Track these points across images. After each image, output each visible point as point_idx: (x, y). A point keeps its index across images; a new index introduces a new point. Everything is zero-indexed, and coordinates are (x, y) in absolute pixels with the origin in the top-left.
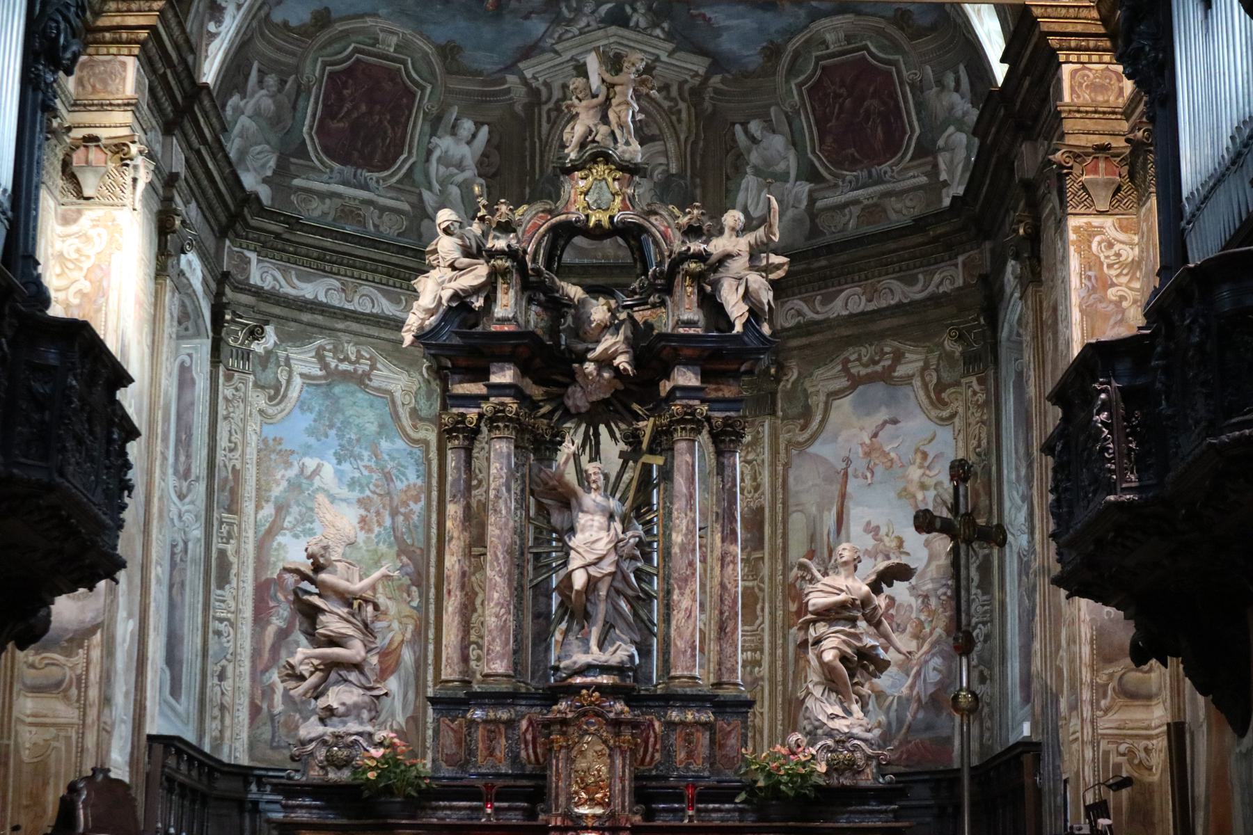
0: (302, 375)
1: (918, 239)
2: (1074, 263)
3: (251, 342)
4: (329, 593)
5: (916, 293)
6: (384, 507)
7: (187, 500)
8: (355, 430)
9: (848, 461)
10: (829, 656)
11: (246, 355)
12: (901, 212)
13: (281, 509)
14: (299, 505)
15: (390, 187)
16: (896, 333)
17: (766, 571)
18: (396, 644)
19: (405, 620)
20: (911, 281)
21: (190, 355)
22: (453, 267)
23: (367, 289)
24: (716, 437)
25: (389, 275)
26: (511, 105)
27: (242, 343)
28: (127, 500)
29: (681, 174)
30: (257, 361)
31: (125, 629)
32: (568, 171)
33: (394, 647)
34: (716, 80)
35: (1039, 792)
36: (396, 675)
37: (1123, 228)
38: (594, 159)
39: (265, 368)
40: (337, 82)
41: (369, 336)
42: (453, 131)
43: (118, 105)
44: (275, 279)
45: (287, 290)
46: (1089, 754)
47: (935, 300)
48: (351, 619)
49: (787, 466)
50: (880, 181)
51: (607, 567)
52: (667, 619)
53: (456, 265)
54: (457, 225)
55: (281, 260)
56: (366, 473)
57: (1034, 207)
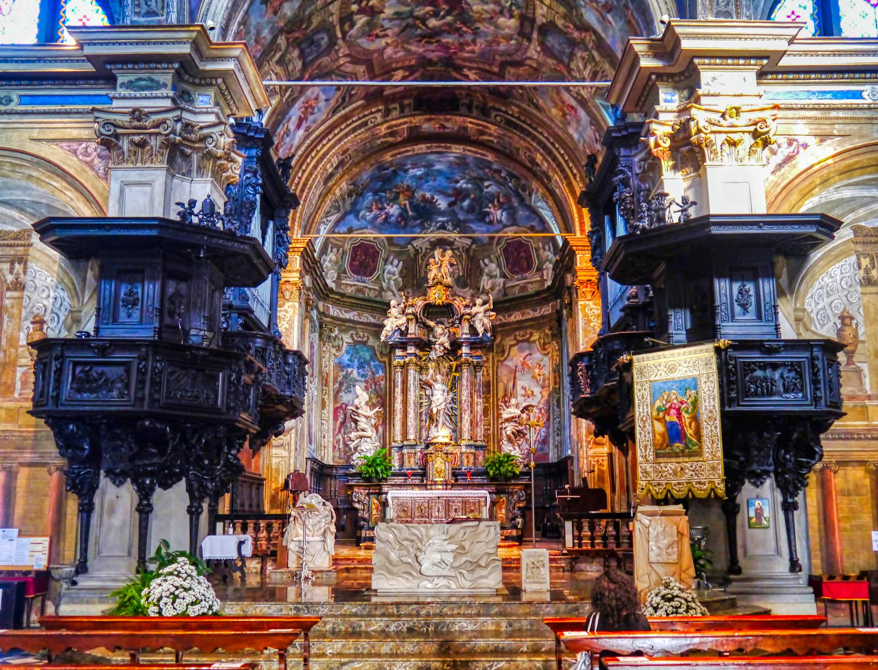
1: (537, 298)
2: (580, 315)
5: (537, 314)
9: (516, 367)
10: (509, 433)
11: (329, 337)
12: (532, 289)
13: (341, 384)
16: (531, 327)
17: (491, 401)
20: (535, 311)
23: (366, 315)
24: (474, 367)
26: (409, 255)
29: (463, 276)
31: (300, 426)
34: (474, 246)
35: (573, 471)
37: (595, 304)
38: (437, 284)
40: (355, 250)
42: (392, 263)
45: (341, 316)
46: (585, 461)
47: (543, 317)
49: (497, 368)
50: (526, 279)
51: (443, 406)
52: (461, 422)
57: (570, 294)
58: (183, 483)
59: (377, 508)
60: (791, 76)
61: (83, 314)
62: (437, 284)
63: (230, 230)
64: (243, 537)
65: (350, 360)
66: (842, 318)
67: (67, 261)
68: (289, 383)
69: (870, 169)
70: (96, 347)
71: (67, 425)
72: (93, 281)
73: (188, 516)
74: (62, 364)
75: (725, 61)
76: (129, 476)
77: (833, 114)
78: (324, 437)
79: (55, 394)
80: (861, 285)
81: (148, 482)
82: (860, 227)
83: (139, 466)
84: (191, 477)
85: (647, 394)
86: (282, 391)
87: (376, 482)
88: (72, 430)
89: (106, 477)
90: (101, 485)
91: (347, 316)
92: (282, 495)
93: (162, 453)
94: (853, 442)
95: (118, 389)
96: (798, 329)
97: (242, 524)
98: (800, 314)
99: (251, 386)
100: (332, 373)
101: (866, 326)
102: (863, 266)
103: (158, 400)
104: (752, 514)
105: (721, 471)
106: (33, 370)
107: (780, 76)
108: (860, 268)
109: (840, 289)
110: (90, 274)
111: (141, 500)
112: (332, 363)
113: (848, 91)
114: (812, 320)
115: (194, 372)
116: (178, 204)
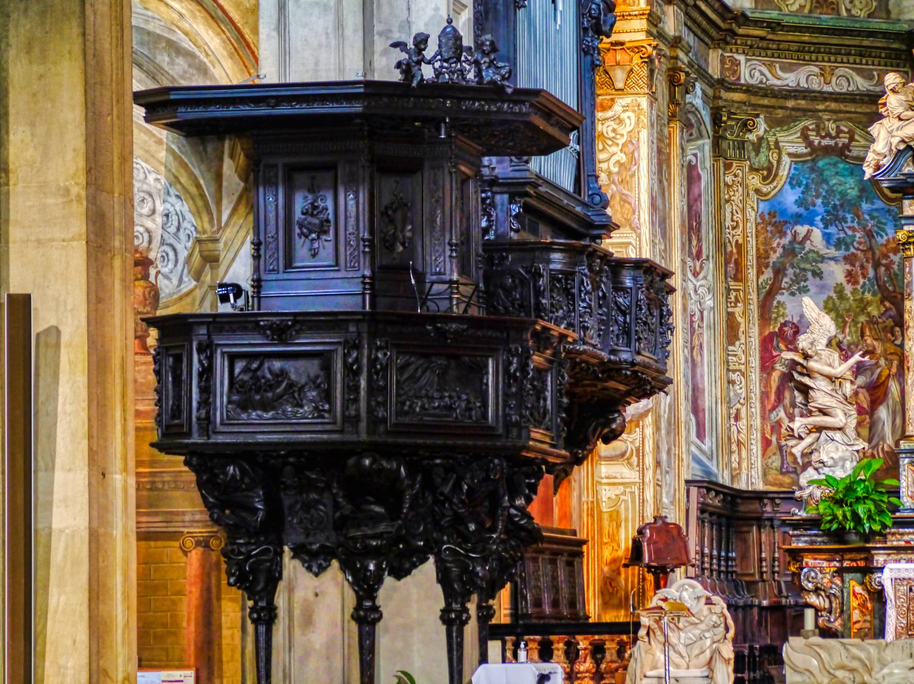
0: (790, 155)
3: (745, 133)
4: (817, 375)
6: (867, 261)
7: (701, 276)
8: (838, 197)
11: (741, 145)
13: (779, 272)
14: (793, 267)
18: (883, 378)
19: (890, 357)
21: (695, 155)
22: (900, 119)
23: (841, 71)
25: (862, 55)
27: (738, 136)
28: (670, 337)
30: (751, 148)
33: (881, 381)
36: (884, 404)
39: (757, 152)
41: (848, 112)
43: (636, 15)
44: (762, 74)
48: (834, 394)
53: (901, 117)
54: (900, 86)
55: (766, 56)
56: (850, 233)
58: (429, 567)
59: (862, 606)
61: (221, 245)
63: (493, 82)
64: (546, 668)
65: (800, 203)
67: (183, 140)
68: (626, 332)
70: (270, 327)
71: (224, 467)
72: (236, 179)
73: (444, 628)
74: (211, 359)
76: (334, 556)
78: (737, 418)
79: (203, 413)
81: (372, 567)
83: (354, 539)
84: (446, 555)
86: (613, 352)
87: (855, 541)
88: (234, 476)
89: (293, 558)
90: (285, 574)
91: (790, 79)
92: (629, 577)
93: (394, 513)
95: (312, 401)
97: (540, 643)
99: (546, 371)
100: (752, 242)
103: (384, 420)
106: (153, 367)
110: (228, 167)
111: (360, 600)
112: (751, 215)
115: (442, 362)
116: (395, 45)
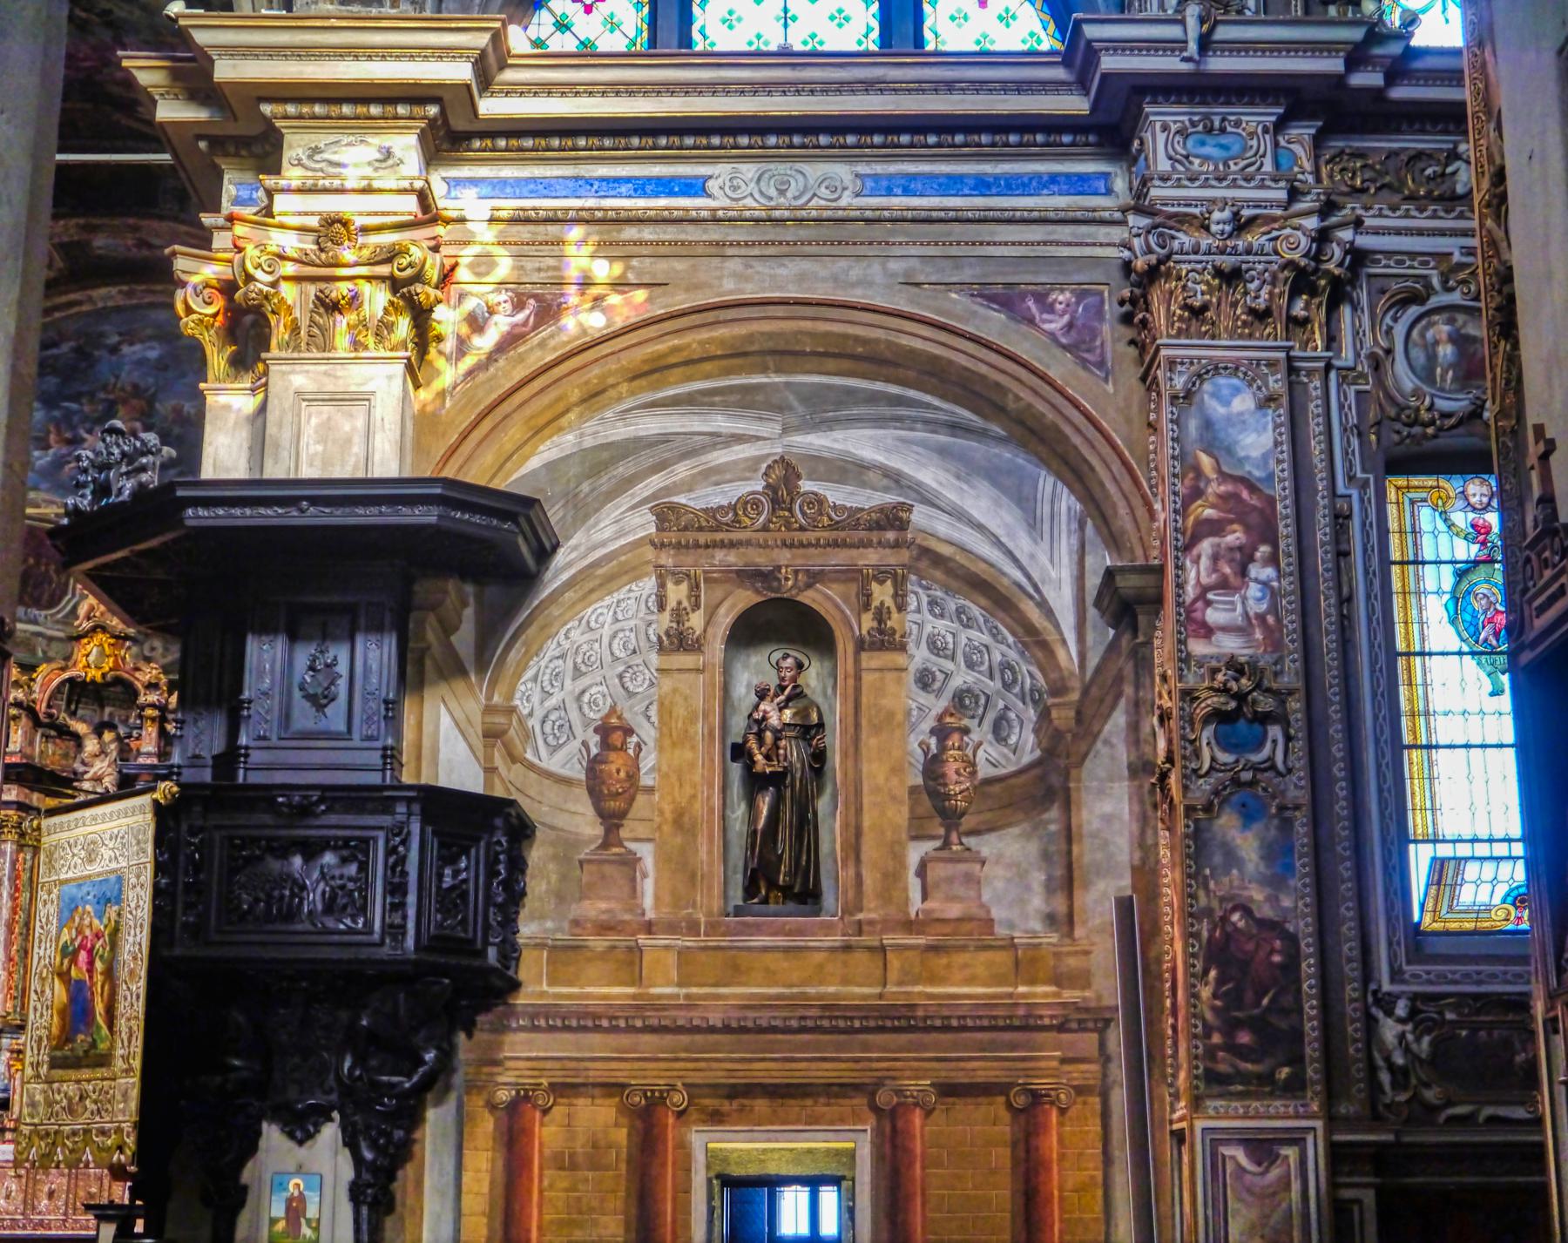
15: (58, 622)
32: (78, 638)
38: (94, 630)
60: (529, 143)
62: (94, 630)
66: (604, 730)
69: (708, 366)
75: (334, 110)
77: (630, 233)
80: (662, 649)
82: (674, 508)
85: (52, 909)
94: (596, 1038)
96: (489, 758)
98: (500, 720)
101: (661, 749)
102: (671, 603)
104: (278, 1210)
105: (133, 1105)
107: (502, 143)
108: (661, 607)
109: (608, 658)
113: (672, 179)
114: (528, 735)
